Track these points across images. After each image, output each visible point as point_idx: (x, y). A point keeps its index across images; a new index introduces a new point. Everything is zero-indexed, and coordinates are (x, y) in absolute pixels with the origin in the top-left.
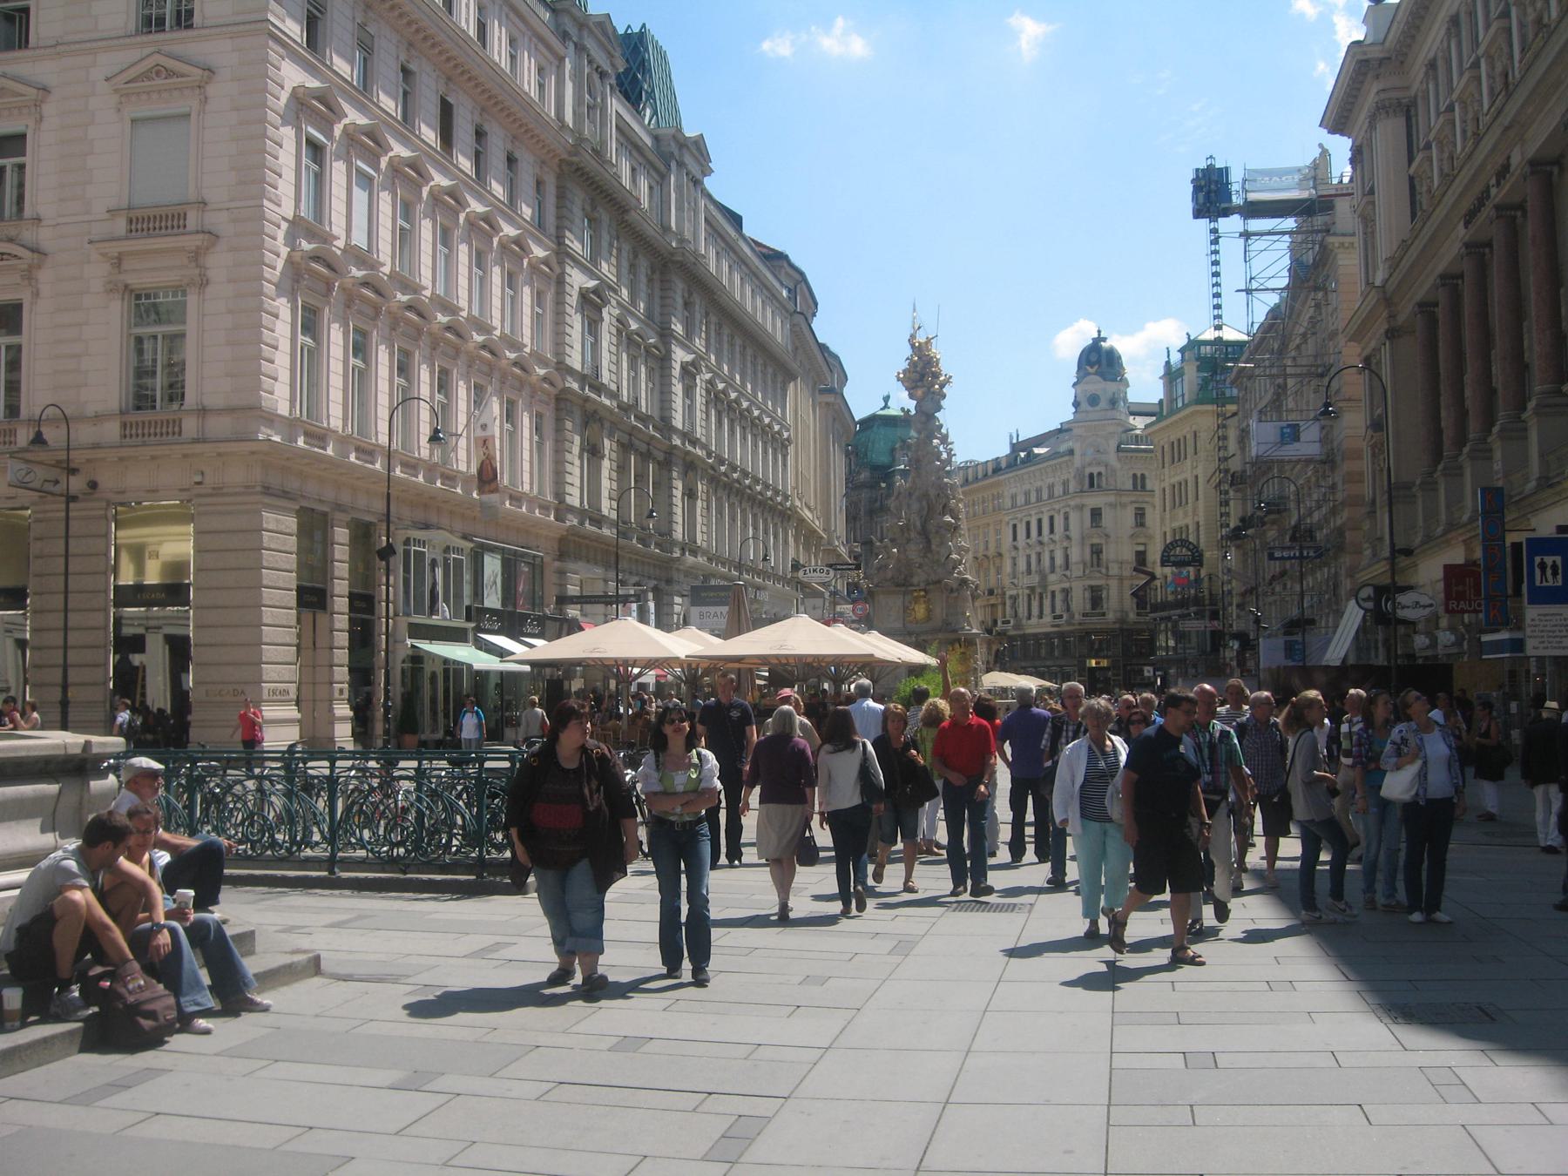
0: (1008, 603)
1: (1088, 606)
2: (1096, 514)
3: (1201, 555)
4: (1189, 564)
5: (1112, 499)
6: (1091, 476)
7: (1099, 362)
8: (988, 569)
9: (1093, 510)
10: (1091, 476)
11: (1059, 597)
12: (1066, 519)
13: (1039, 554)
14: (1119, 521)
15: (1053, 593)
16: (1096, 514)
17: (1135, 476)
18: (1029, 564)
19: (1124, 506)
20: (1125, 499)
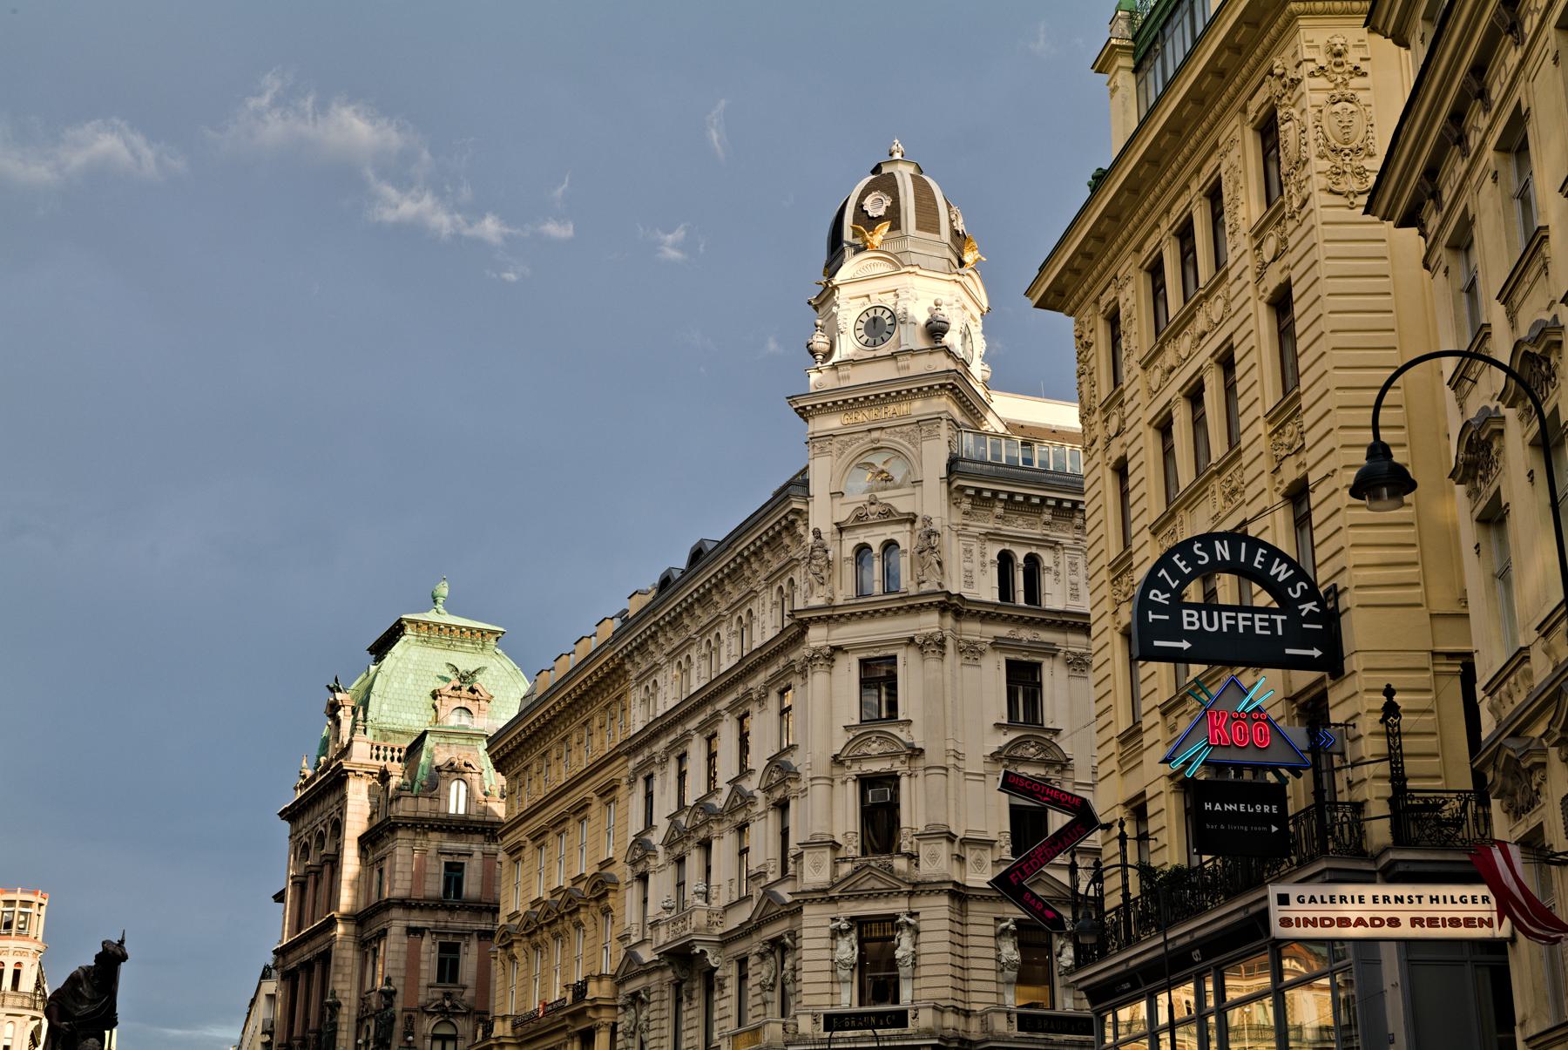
0: (625, 1021)
1: (847, 999)
2: (878, 676)
3: (1331, 618)
4: (1264, 654)
5: (930, 623)
6: (862, 550)
7: (893, 216)
8: (578, 925)
9: (864, 663)
10: (862, 550)
11: (760, 972)
12: (784, 712)
13: (706, 845)
14: (954, 704)
15: (742, 962)
16: (878, 676)
17: (1005, 560)
18: (681, 885)
19: (971, 651)
20: (973, 630)
